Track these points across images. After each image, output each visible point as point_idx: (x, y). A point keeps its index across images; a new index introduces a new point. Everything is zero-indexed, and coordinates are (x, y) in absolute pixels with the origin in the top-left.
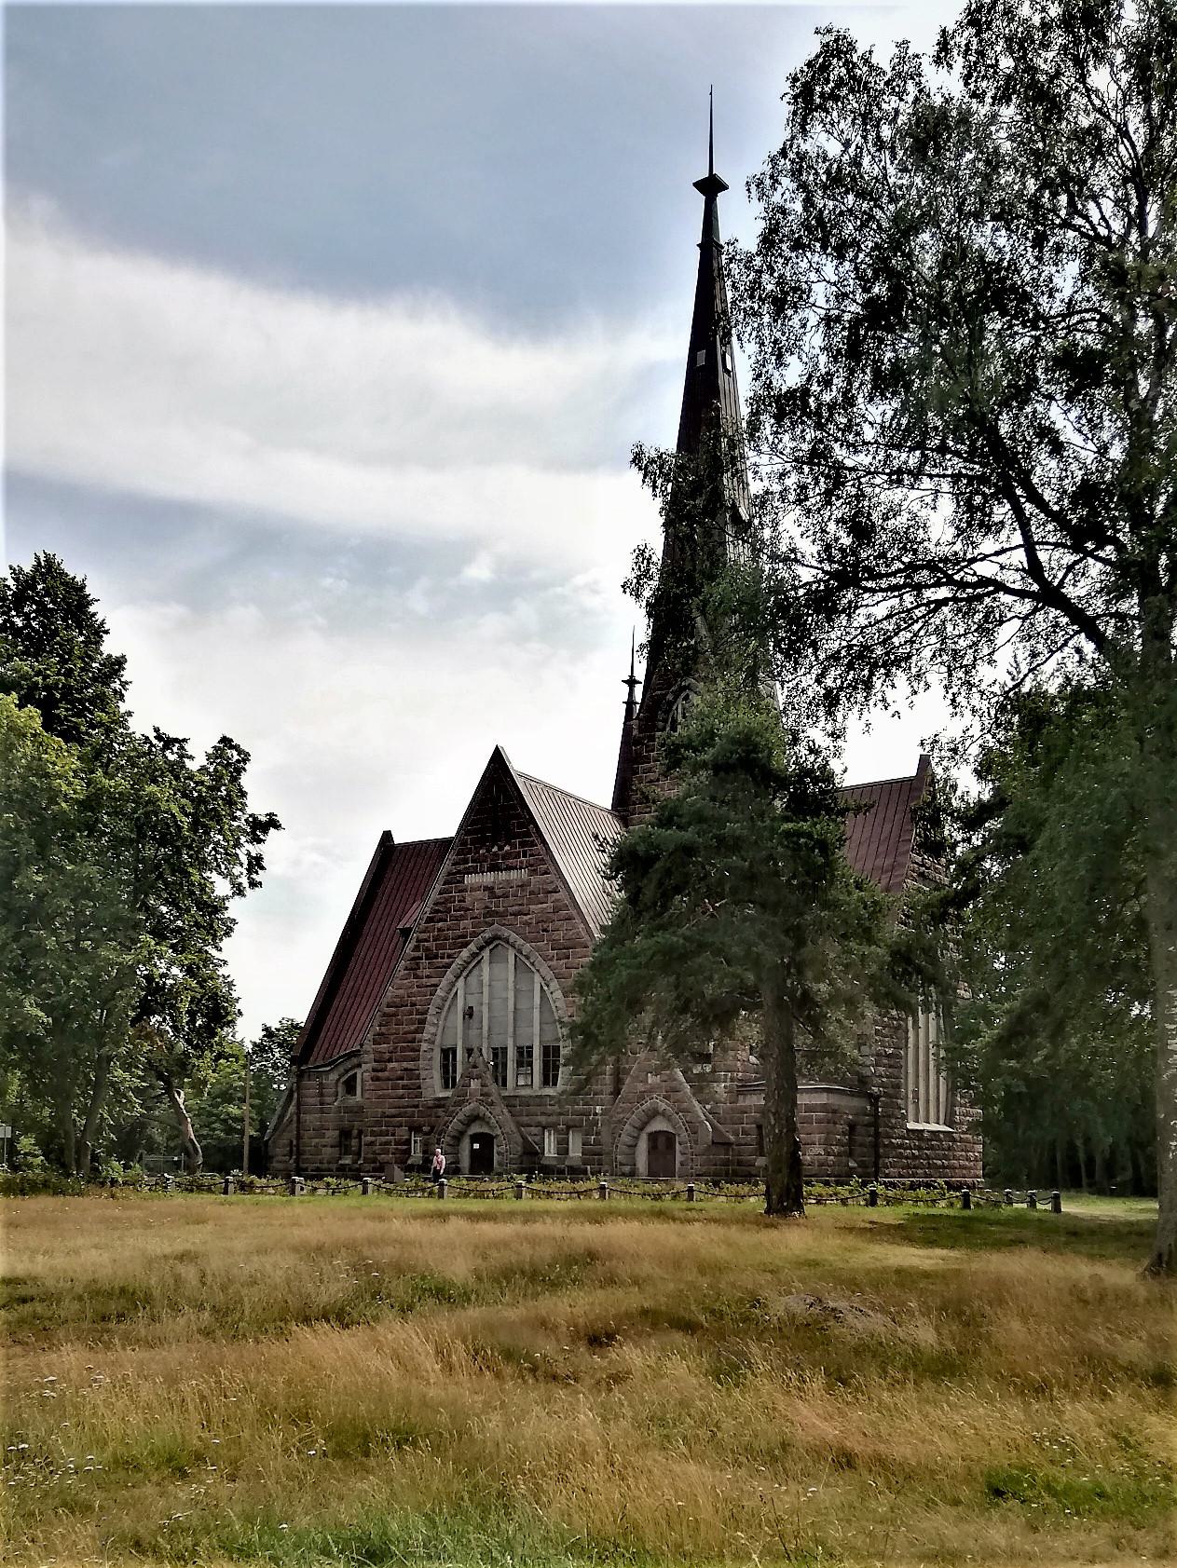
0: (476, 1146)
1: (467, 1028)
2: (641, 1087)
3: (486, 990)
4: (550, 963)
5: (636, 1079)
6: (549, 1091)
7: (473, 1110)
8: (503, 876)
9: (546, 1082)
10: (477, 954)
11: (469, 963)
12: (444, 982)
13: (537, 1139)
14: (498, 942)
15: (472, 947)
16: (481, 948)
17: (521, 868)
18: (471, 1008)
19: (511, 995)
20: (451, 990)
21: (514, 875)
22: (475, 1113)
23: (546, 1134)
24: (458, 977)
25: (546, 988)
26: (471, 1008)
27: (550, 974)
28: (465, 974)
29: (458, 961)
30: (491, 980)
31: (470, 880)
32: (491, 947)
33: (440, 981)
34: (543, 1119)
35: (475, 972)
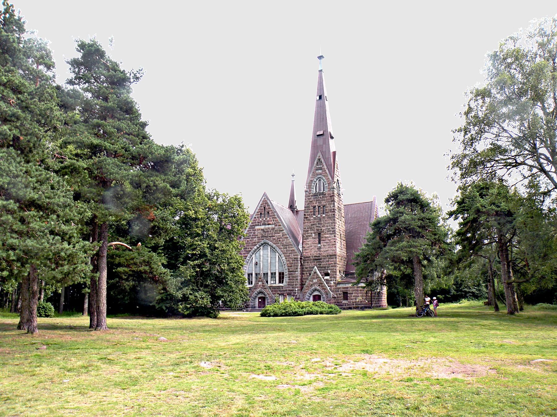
0: (260, 300)
1: (256, 268)
2: (311, 283)
3: (261, 257)
5: (310, 281)
6: (281, 285)
8: (267, 226)
9: (280, 282)
12: (249, 255)
16: (260, 246)
18: (257, 262)
19: (269, 259)
21: (270, 226)
24: (253, 254)
26: (257, 262)
29: (253, 249)
30: (263, 255)
31: (257, 227)
35: (258, 252)
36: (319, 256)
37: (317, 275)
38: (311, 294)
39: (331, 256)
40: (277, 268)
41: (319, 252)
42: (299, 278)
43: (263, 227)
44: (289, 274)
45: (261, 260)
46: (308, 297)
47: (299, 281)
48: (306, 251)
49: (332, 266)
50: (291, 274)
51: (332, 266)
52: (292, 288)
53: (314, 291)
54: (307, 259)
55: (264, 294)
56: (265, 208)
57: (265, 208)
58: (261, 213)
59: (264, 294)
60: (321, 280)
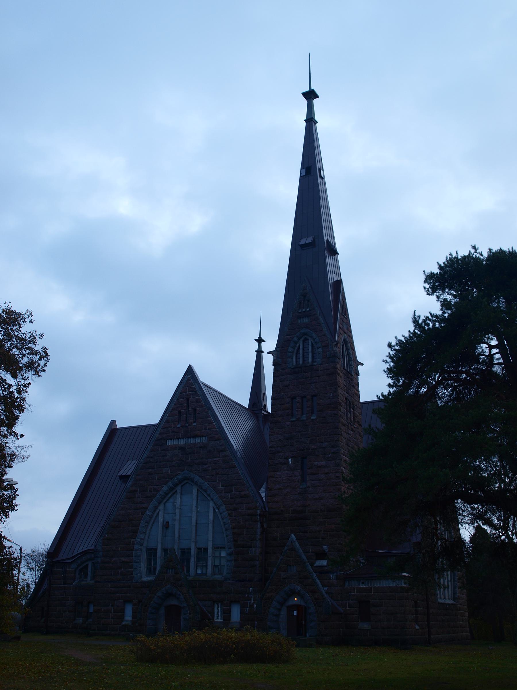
3: (178, 511)
8: (191, 441)
14: (185, 481)
15: (170, 484)
17: (203, 437)
18: (168, 523)
19: (194, 514)
21: (198, 440)
24: (160, 503)
25: (217, 510)
26: (168, 523)
28: (164, 501)
29: (161, 493)
30: (181, 505)
31: (170, 443)
32: (182, 484)
35: (171, 500)
40: (210, 537)
43: (183, 442)
56: (188, 399)
57: (188, 399)
58: (180, 412)
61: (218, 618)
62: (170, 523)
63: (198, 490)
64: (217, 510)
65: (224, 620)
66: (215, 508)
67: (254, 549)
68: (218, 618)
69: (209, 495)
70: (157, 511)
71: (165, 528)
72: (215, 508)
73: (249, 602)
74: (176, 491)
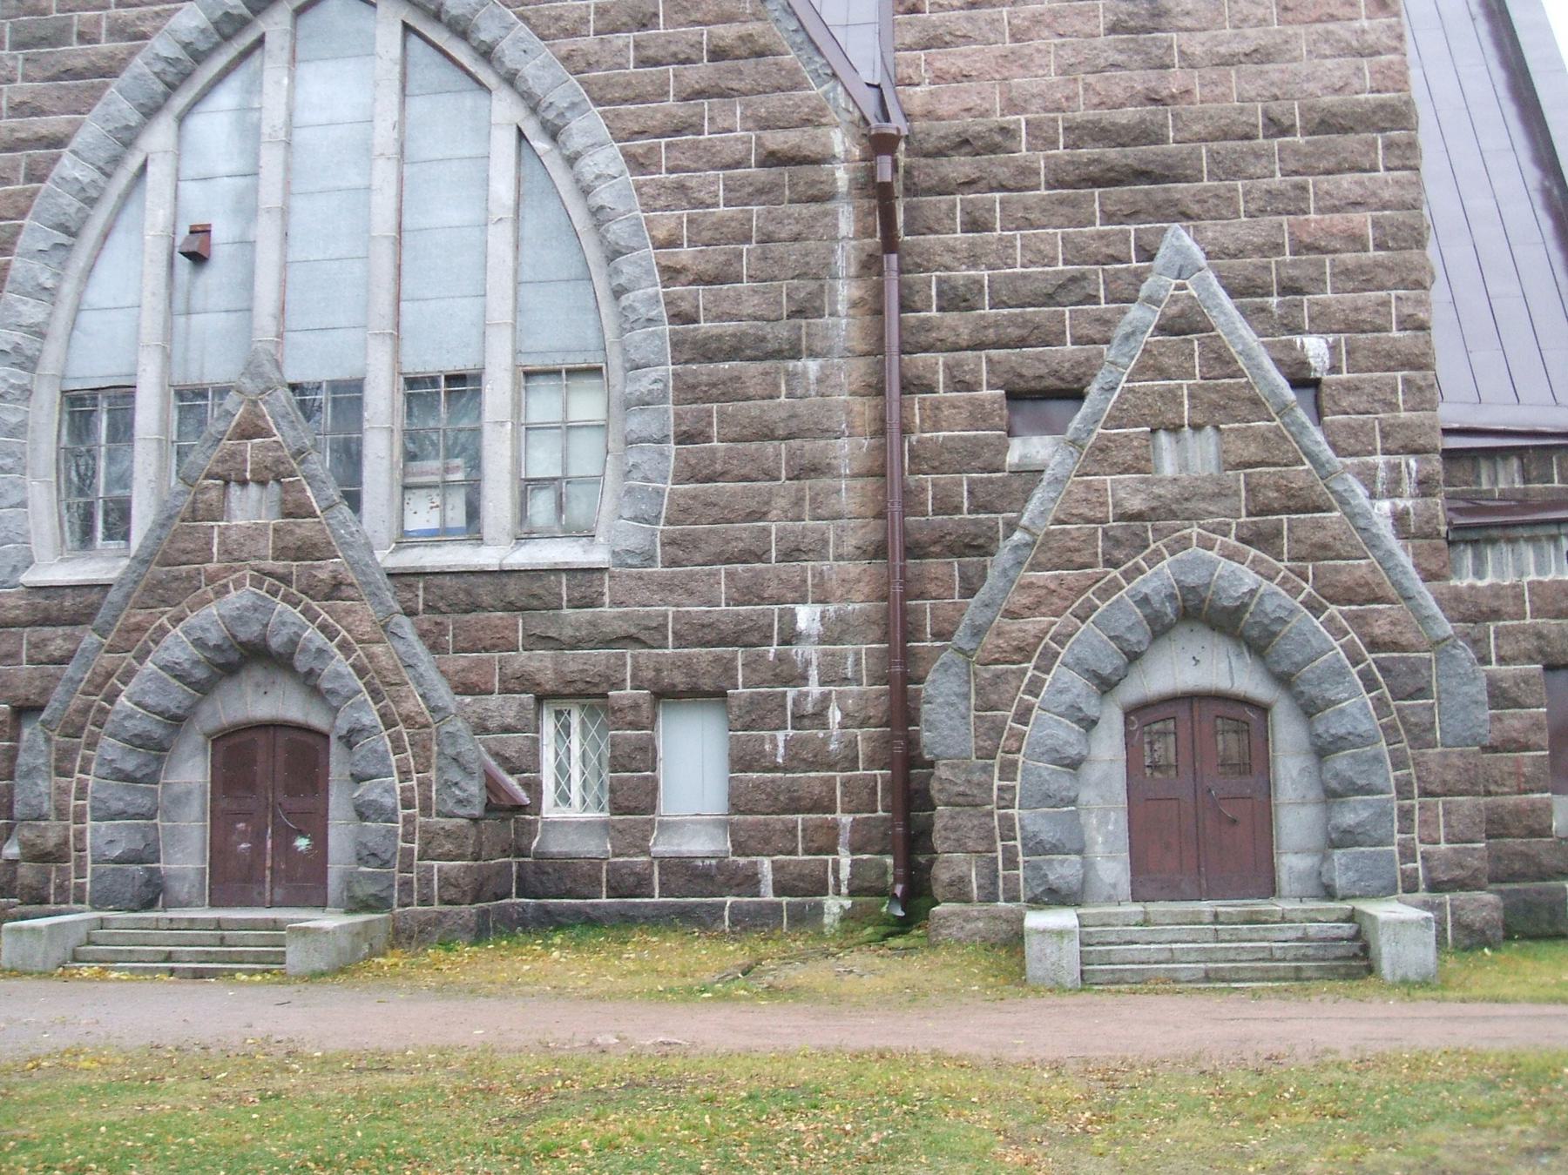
3: (271, 160)
4: (565, 45)
7: (233, 621)
10: (242, 24)
11: (199, 57)
12: (91, 131)
13: (514, 743)
18: (201, 231)
20: (116, 160)
22: (248, 633)
23: (549, 726)
24: (150, 111)
26: (201, 231)
27: (561, 90)
28: (180, 101)
29: (162, 46)
33: (77, 126)
34: (541, 663)
35: (226, 98)
36: (1146, 134)
37: (1221, 360)
38: (1106, 685)
39: (1326, 124)
40: (500, 308)
41: (1141, 79)
42: (848, 451)
44: (687, 391)
45: (270, 193)
46: (1065, 733)
47: (848, 494)
48: (946, 60)
49: (1362, 278)
50: (729, 391)
51: (1362, 278)
52: (749, 593)
53: (1160, 630)
54: (960, 166)
55: (310, 683)
59: (310, 683)
60: (1276, 449)
61: (564, 798)
62: (221, 234)
63: (407, 28)
64: (541, 145)
65: (616, 809)
66: (531, 129)
67: (812, 366)
68: (564, 798)
69: (486, 54)
70: (134, 163)
71: (183, 263)
72: (531, 129)
73: (791, 693)
74: (260, 42)
